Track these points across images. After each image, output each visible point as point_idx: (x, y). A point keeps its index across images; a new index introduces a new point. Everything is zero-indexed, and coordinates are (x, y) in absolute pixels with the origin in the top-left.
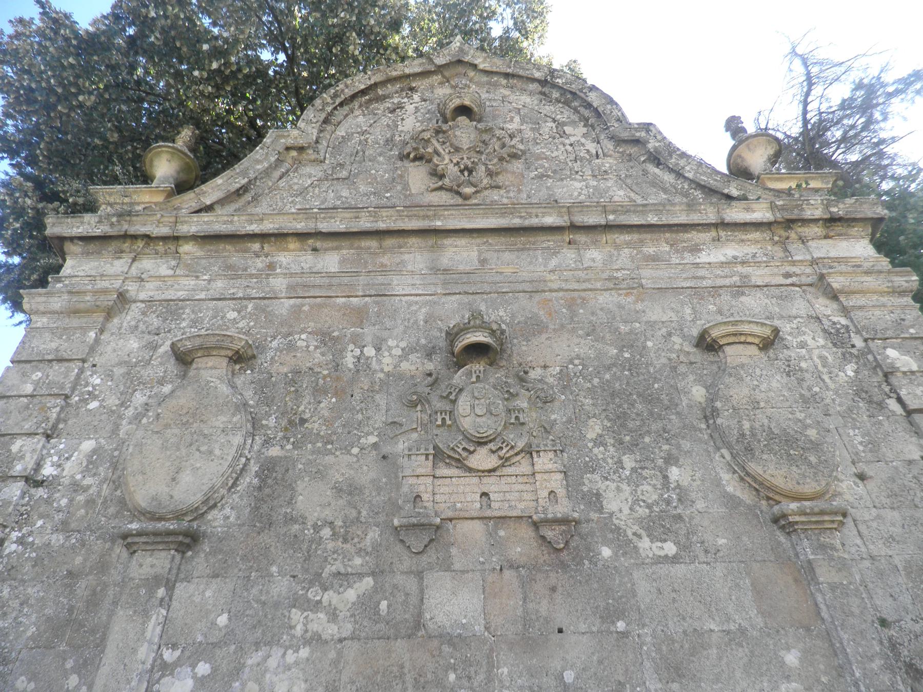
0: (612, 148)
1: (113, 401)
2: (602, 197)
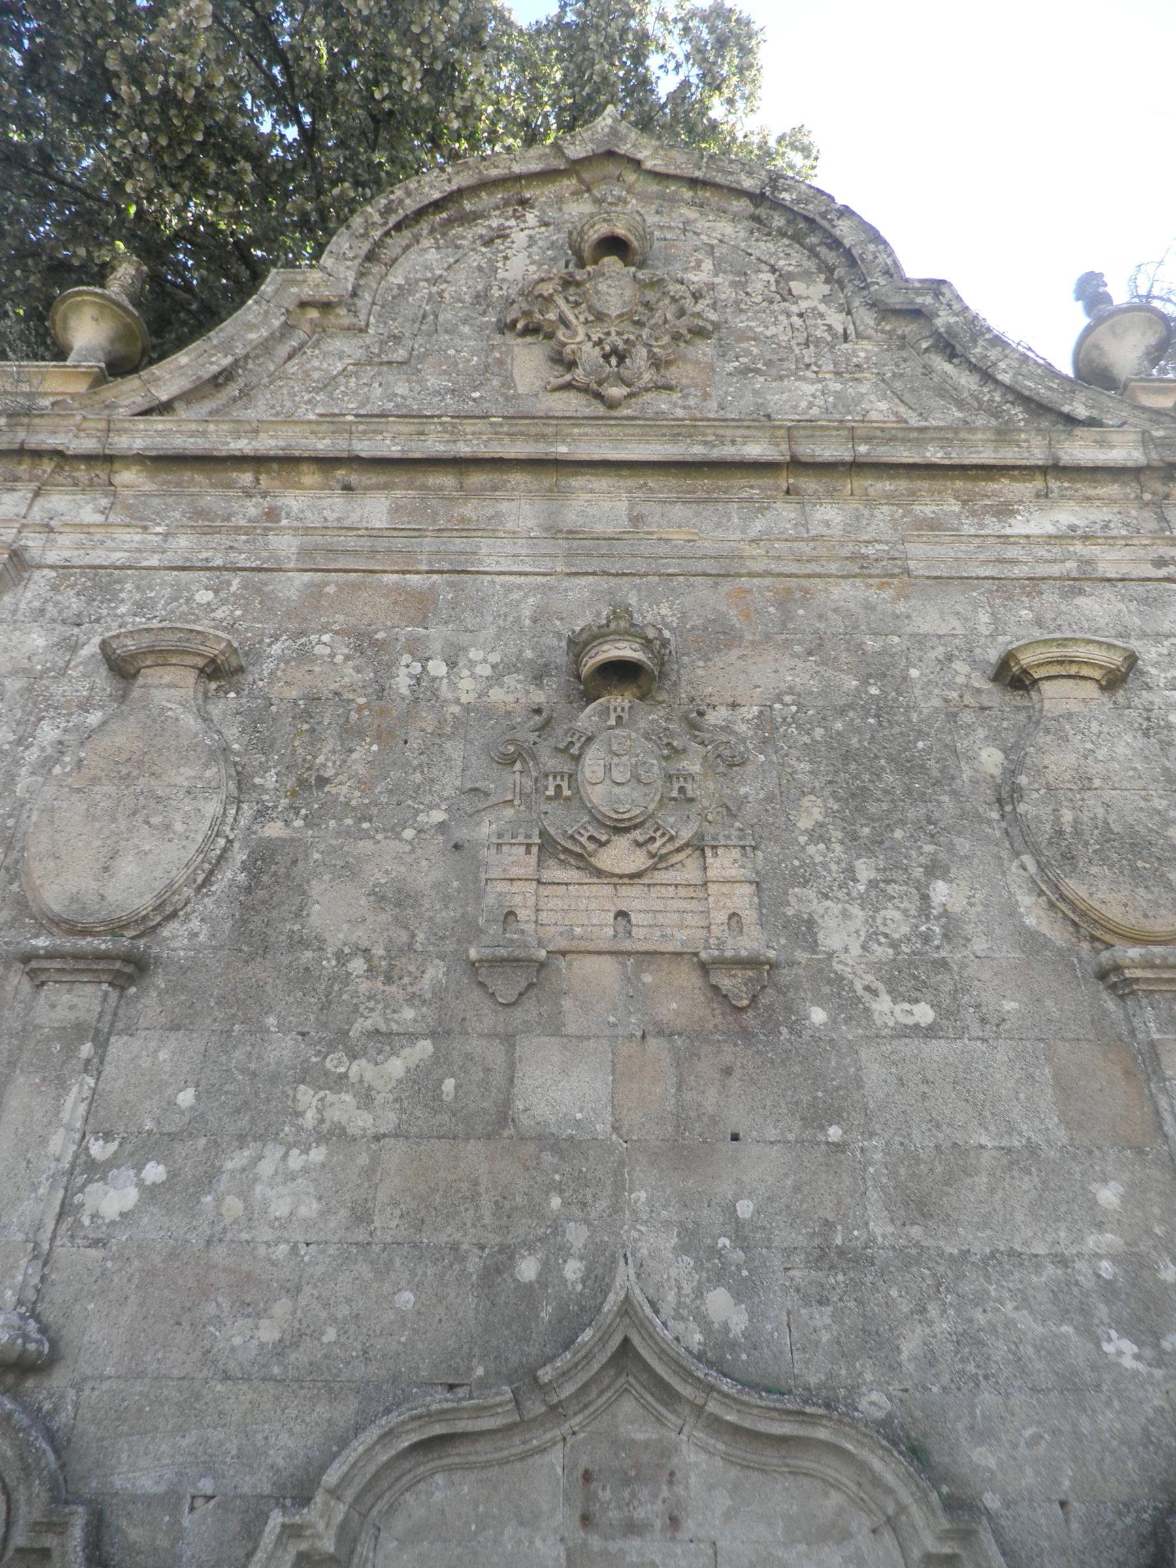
0: (872, 323)
2: (849, 413)
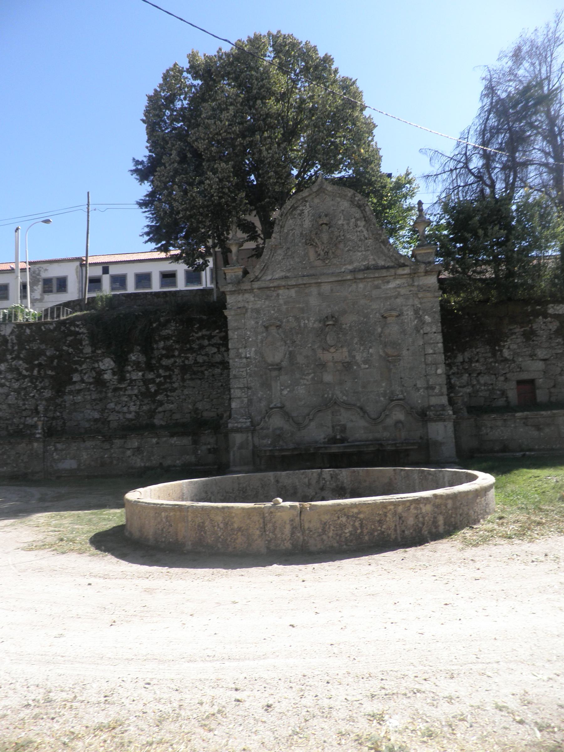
1: (254, 338)
